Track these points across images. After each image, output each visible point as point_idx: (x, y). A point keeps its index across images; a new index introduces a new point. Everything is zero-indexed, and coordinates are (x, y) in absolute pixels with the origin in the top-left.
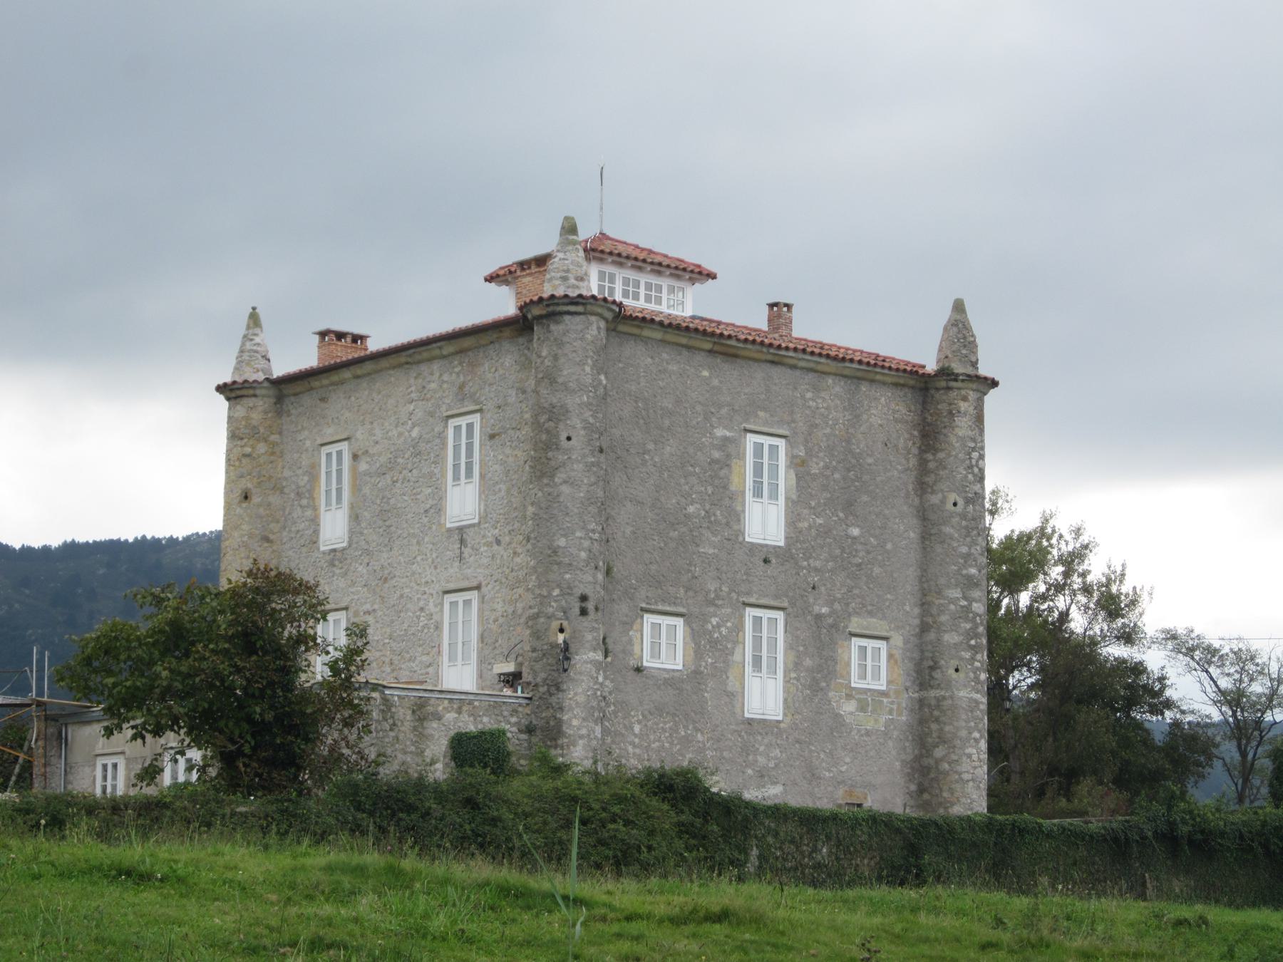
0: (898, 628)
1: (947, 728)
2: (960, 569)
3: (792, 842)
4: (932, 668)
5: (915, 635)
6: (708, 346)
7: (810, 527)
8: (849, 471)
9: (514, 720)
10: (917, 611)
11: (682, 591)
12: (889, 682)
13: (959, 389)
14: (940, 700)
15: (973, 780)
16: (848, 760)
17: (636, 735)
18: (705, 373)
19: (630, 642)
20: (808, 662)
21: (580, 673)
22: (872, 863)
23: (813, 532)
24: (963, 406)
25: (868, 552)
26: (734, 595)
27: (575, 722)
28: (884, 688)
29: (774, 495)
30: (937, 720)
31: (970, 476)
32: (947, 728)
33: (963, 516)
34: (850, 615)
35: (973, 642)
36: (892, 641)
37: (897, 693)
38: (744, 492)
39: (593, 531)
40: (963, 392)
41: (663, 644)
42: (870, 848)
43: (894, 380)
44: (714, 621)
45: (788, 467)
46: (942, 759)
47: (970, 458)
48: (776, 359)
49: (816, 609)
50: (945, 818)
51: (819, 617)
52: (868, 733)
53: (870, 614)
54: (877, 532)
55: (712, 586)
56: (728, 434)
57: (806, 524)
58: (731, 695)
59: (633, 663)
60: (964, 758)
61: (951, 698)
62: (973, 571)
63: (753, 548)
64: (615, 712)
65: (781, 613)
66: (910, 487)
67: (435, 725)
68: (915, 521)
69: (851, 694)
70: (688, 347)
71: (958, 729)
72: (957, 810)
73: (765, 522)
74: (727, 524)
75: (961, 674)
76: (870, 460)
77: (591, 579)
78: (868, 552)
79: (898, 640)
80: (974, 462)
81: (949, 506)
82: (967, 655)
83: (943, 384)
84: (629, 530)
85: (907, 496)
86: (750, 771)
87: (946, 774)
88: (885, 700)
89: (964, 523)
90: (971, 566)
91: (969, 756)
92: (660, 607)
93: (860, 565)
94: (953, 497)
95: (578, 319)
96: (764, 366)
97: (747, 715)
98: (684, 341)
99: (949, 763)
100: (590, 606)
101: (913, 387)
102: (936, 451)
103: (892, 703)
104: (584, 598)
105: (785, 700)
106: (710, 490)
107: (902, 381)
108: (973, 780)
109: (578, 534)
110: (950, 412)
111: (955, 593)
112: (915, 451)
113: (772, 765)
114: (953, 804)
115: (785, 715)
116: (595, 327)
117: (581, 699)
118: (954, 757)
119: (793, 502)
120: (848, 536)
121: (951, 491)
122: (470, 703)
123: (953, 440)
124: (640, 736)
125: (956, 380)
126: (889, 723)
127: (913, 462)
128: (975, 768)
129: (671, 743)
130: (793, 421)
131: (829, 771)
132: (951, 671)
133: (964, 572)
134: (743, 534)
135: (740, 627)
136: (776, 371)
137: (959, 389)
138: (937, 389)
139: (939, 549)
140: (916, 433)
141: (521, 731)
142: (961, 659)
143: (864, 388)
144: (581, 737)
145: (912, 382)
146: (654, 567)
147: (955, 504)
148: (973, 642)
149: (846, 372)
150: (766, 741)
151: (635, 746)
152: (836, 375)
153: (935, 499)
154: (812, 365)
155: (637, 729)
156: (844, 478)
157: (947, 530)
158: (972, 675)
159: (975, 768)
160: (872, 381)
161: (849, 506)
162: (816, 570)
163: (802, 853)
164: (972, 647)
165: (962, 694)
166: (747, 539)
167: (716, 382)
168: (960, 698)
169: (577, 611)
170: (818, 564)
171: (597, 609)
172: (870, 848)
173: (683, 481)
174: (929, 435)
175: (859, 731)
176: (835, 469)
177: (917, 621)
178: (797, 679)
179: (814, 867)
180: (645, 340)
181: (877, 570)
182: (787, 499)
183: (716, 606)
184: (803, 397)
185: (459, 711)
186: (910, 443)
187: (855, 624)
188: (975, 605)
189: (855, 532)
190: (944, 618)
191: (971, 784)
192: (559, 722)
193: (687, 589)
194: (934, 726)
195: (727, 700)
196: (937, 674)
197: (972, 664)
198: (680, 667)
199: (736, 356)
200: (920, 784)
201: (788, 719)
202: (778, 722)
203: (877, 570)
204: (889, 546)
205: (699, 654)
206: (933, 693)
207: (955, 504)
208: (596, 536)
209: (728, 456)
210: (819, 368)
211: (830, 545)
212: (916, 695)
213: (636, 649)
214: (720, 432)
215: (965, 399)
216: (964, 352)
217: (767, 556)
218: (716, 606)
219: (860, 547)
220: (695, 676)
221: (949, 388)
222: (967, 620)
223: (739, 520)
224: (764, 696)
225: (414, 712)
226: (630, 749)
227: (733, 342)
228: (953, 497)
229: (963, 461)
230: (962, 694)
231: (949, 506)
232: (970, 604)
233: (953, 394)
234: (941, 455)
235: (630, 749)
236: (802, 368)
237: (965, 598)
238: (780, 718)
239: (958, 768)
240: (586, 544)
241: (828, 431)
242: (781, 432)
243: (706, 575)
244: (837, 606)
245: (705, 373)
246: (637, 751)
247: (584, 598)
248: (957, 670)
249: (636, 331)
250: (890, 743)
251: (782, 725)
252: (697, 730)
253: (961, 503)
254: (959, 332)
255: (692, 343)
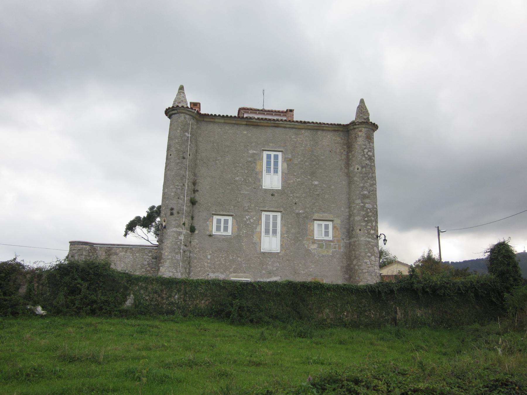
0: (338, 217)
1: (357, 253)
2: (360, 192)
3: (156, 292)
4: (352, 230)
5: (347, 219)
6: (245, 123)
7: (294, 182)
8: (313, 161)
9: (150, 254)
10: (347, 210)
11: (232, 207)
12: (333, 237)
13: (358, 128)
14: (355, 242)
15: (367, 272)
16: (313, 266)
17: (208, 259)
18: (245, 132)
19: (207, 226)
20: (293, 231)
21: (169, 236)
22: (207, 303)
23: (296, 184)
24: (360, 134)
25: (322, 190)
26: (257, 208)
27: (166, 254)
28: (331, 239)
29: (276, 171)
30: (354, 250)
31: (364, 158)
32: (357, 253)
33: (361, 173)
34: (313, 213)
35: (366, 219)
36: (335, 222)
37: (338, 241)
38: (262, 171)
39: (178, 186)
40: (360, 129)
41: (222, 226)
42: (206, 296)
43: (332, 129)
44: (247, 217)
45: (283, 162)
46: (355, 265)
47: (364, 152)
48: (276, 125)
49: (297, 211)
50: (356, 286)
51: (298, 214)
52: (323, 256)
53: (324, 212)
54: (327, 182)
55: (246, 205)
56: (255, 152)
57: (292, 181)
58: (255, 244)
59: (208, 233)
60: (364, 264)
61: (358, 241)
62: (365, 192)
63: (266, 190)
64: (199, 251)
65: (280, 213)
66: (343, 166)
67: (115, 257)
68: (345, 178)
69: (314, 242)
70: (237, 124)
71: (361, 252)
72: (361, 284)
73: (272, 181)
74: (254, 183)
75: (362, 232)
76: (323, 157)
77: (176, 202)
78: (322, 190)
79: (338, 221)
80: (365, 153)
81: (356, 170)
82: (364, 224)
83: (352, 127)
84: (208, 187)
85: (341, 169)
86: (264, 272)
87: (357, 270)
88: (332, 244)
89: (361, 175)
90: (365, 191)
91: (366, 263)
92: (221, 213)
93: (319, 194)
94: (357, 166)
95: (176, 115)
96: (271, 128)
97: (262, 251)
98: (234, 122)
99: (358, 266)
100: (175, 212)
101: (342, 131)
102: (352, 151)
103: (336, 244)
104: (172, 209)
105: (281, 245)
106: (246, 171)
107: (336, 129)
108: (367, 272)
109: (171, 187)
110: (356, 137)
111: (358, 201)
112: (345, 153)
113: (275, 269)
114: (359, 282)
115: (281, 250)
116: (183, 117)
117: (169, 245)
118: (359, 264)
119: (286, 174)
120: (312, 185)
121: (356, 164)
122: (131, 249)
123: (356, 146)
124: (211, 259)
125: (356, 125)
126: (333, 253)
127: (344, 157)
128: (369, 267)
129: (226, 262)
130: (286, 146)
131: (304, 271)
132: (358, 231)
133: (362, 193)
134: (262, 186)
135: (260, 219)
136: (278, 130)
137: (358, 128)
138: (351, 130)
139: (353, 186)
140: (345, 147)
141: (153, 258)
142: (361, 226)
143: (319, 133)
144: (168, 259)
145: (341, 129)
146: (219, 199)
147: (358, 169)
148: (366, 219)
149: (309, 127)
150: (272, 260)
151: (208, 263)
152: (304, 129)
153: (351, 169)
154: (292, 126)
155: (209, 257)
156: (310, 164)
157: (355, 179)
158: (366, 231)
159: (369, 267)
160: (323, 130)
161: (313, 174)
162: (297, 197)
163: (162, 298)
164: (366, 221)
165: (362, 239)
166: (263, 188)
167: (250, 135)
168: (361, 241)
169: (169, 214)
170: (298, 195)
171: (178, 213)
172: (206, 296)
173: (234, 169)
174: (349, 146)
175: (318, 255)
176: (306, 161)
177: (348, 214)
178: (288, 237)
179: (169, 304)
180: (218, 123)
181: (327, 196)
182: (282, 173)
183: (248, 212)
184: (290, 137)
185: (126, 252)
186: (342, 151)
187: (316, 216)
188: (367, 205)
189: (316, 183)
190: (355, 211)
191: (367, 274)
192: (161, 254)
193: (234, 206)
194: (353, 252)
195: (253, 245)
196: (354, 233)
197: (366, 227)
198: (230, 234)
199: (258, 126)
200: (350, 275)
201: (283, 252)
202: (279, 253)
203: (327, 196)
204: (333, 187)
205: (239, 229)
206: (353, 240)
207: (358, 169)
208: (179, 187)
209: (255, 159)
210: (296, 127)
211: (304, 188)
212: (348, 241)
213: (210, 228)
214: (251, 152)
215: (361, 131)
216: (361, 115)
217: (273, 193)
218: (248, 212)
219: (318, 188)
220: (237, 237)
221: (355, 129)
222: (363, 210)
223: (260, 181)
224: (271, 243)
225: (106, 252)
226: (206, 264)
227: (254, 120)
228: (357, 166)
229: (361, 153)
230: (362, 239)
231: (356, 170)
232: (365, 205)
233: (356, 130)
234: (353, 153)
235: (206, 264)
236: (289, 128)
237: (362, 203)
238: (279, 251)
239: (361, 268)
240: (174, 190)
241: (302, 148)
242: (280, 150)
243: (247, 202)
244: (307, 210)
245: (245, 132)
246: (209, 265)
247: (172, 209)
248: (360, 230)
249: (212, 120)
250: (335, 260)
251: (280, 254)
252: (238, 257)
253: (360, 168)
254: (362, 109)
255: (237, 122)
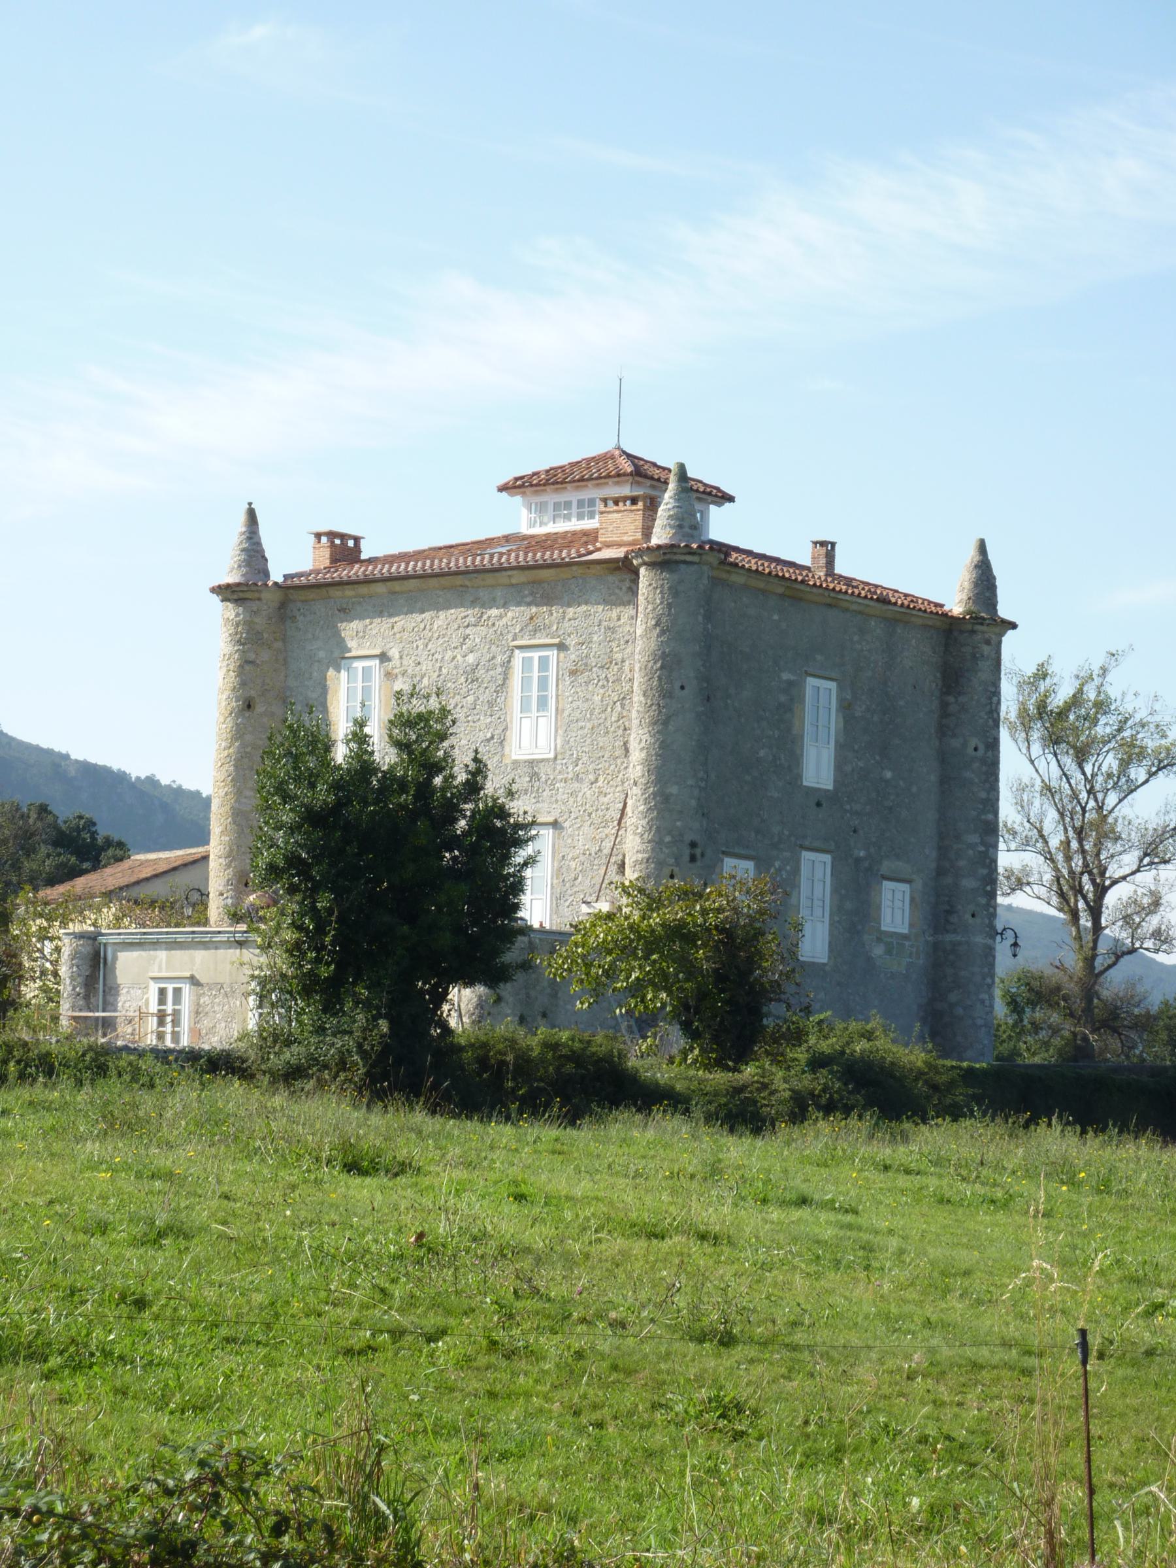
4: (949, 912)
6: (780, 590)
10: (934, 854)
11: (753, 834)
20: (848, 905)
26: (793, 839)
28: (906, 931)
44: (777, 864)
45: (837, 711)
51: (858, 860)
55: (776, 829)
63: (811, 791)
69: (881, 937)
73: (818, 767)
75: (978, 920)
76: (902, 703)
79: (919, 884)
81: (970, 751)
88: (907, 943)
89: (984, 768)
91: (983, 1002)
94: (974, 742)
105: (830, 943)
110: (974, 656)
115: (829, 958)
125: (982, 624)
132: (968, 916)
135: (796, 871)
140: (938, 675)
147: (976, 749)
153: (956, 743)
154: (861, 608)
157: (968, 774)
167: (784, 625)
169: (686, 858)
177: (933, 865)
182: (837, 742)
189: (888, 775)
190: (962, 863)
196: (954, 919)
197: (987, 910)
202: (824, 964)
206: (949, 938)
207: (976, 749)
209: (792, 700)
212: (930, 939)
214: (785, 676)
217: (819, 799)
231: (970, 751)
234: (962, 699)
237: (983, 843)
242: (833, 675)
245: (776, 617)
248: (973, 916)
253: (981, 747)
